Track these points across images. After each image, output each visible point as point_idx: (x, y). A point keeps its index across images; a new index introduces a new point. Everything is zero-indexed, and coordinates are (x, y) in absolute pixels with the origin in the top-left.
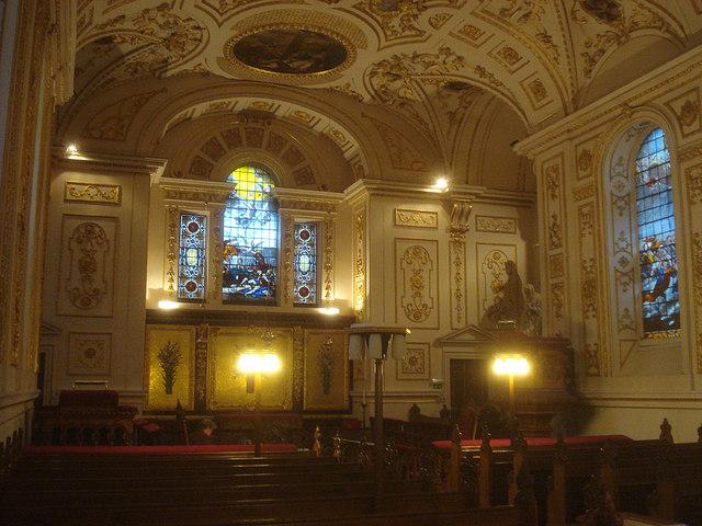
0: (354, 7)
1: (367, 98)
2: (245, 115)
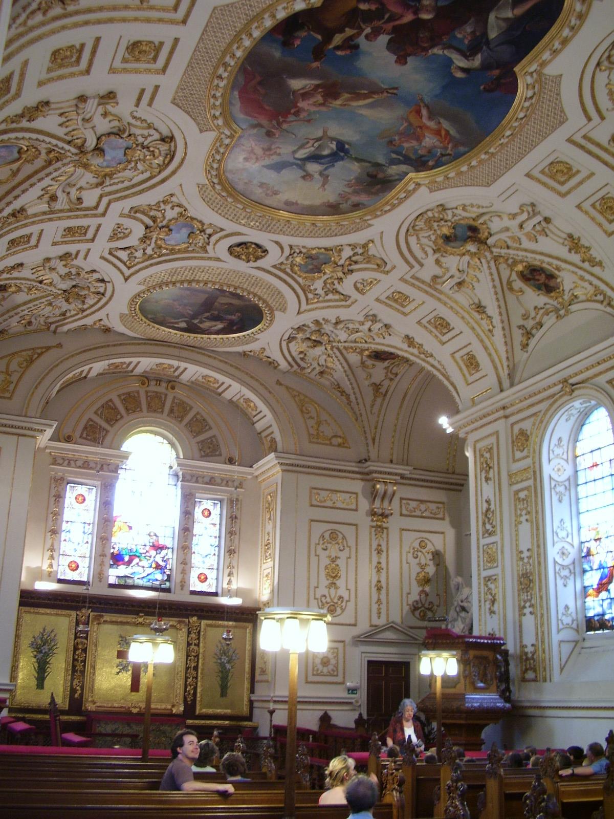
0: (274, 266)
1: (283, 365)
2: (145, 378)
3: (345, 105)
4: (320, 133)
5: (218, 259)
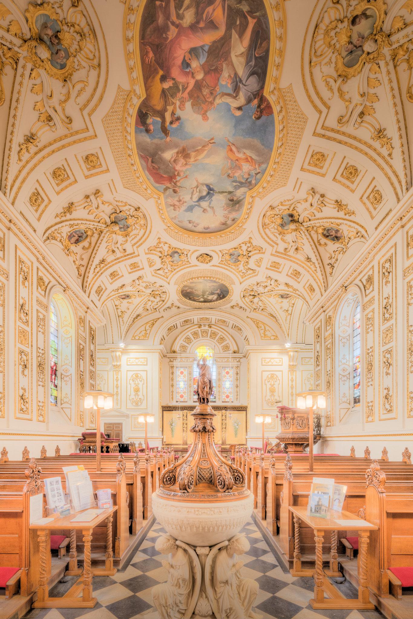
3: (196, 160)
4: (195, 184)
5: (197, 266)
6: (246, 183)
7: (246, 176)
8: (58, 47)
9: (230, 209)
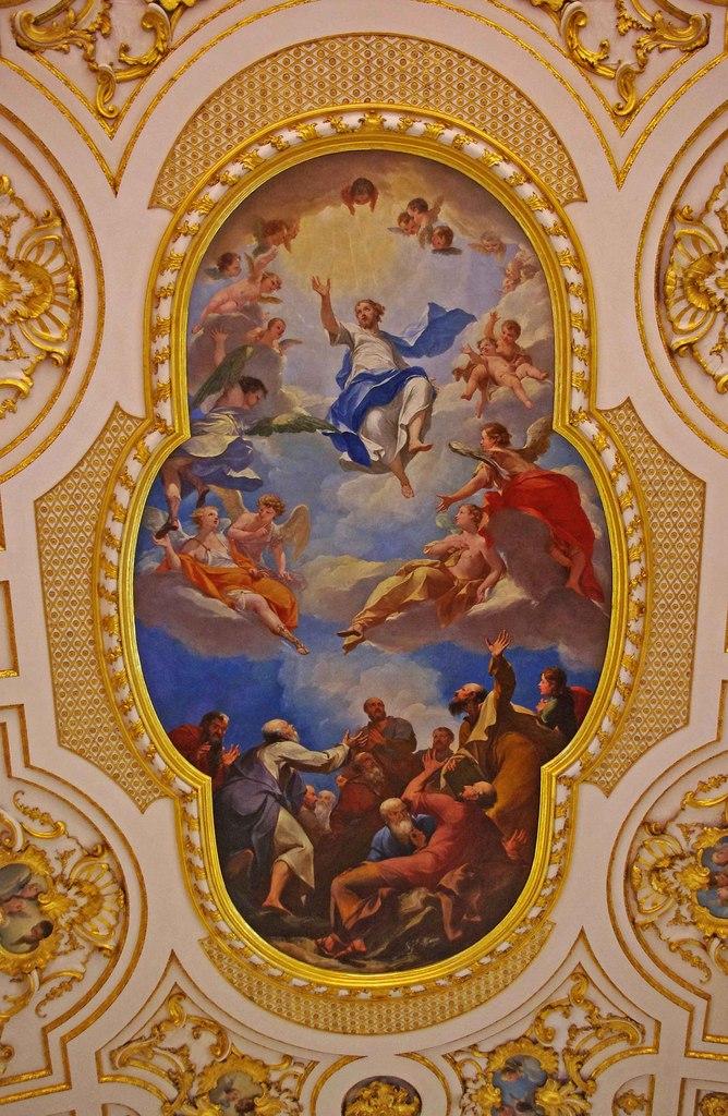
3: (409, 570)
4: (413, 469)
6: (205, 480)
7: (210, 513)
8: (719, 869)
9: (251, 335)
